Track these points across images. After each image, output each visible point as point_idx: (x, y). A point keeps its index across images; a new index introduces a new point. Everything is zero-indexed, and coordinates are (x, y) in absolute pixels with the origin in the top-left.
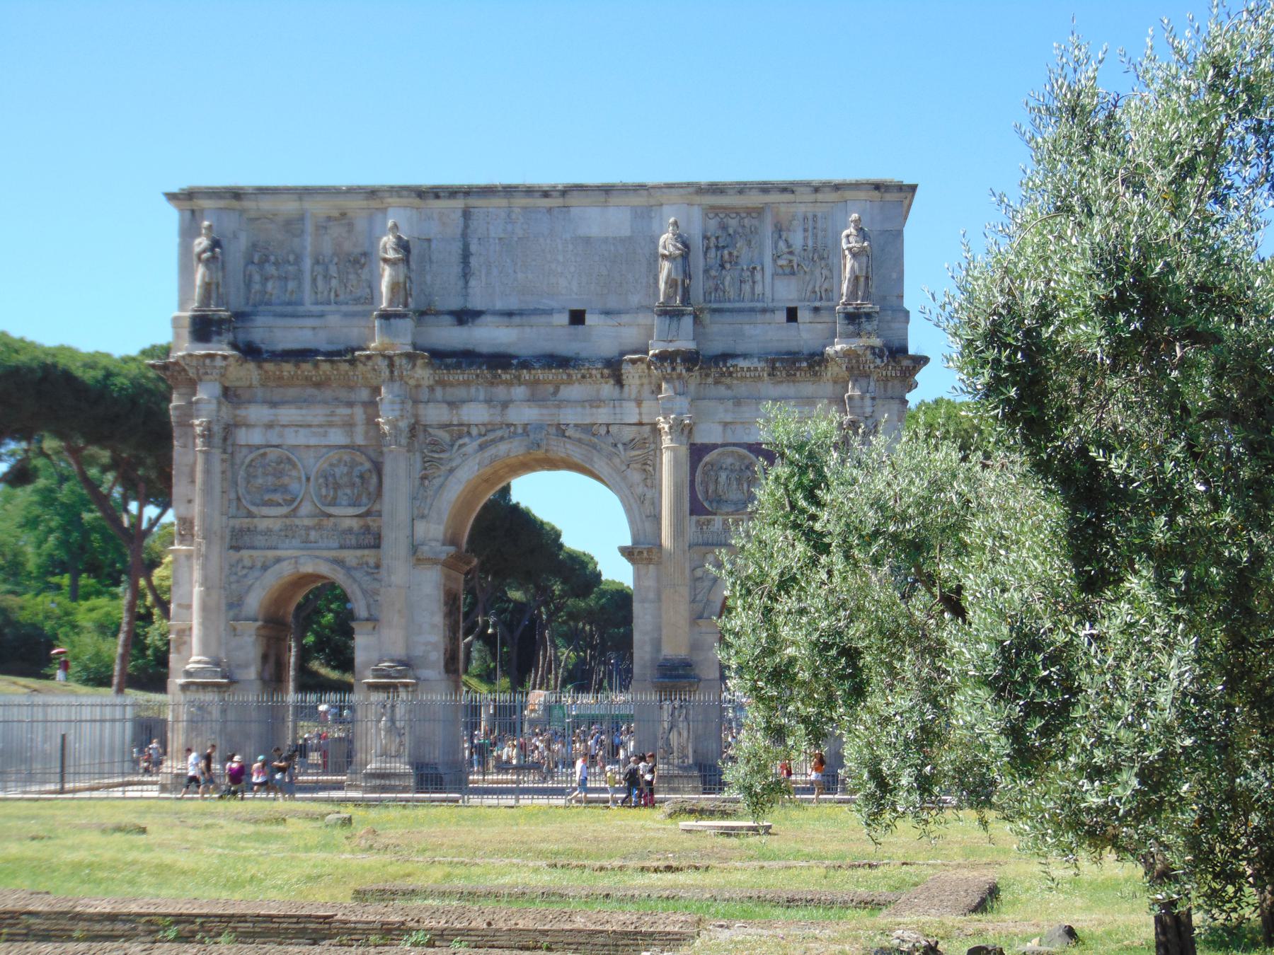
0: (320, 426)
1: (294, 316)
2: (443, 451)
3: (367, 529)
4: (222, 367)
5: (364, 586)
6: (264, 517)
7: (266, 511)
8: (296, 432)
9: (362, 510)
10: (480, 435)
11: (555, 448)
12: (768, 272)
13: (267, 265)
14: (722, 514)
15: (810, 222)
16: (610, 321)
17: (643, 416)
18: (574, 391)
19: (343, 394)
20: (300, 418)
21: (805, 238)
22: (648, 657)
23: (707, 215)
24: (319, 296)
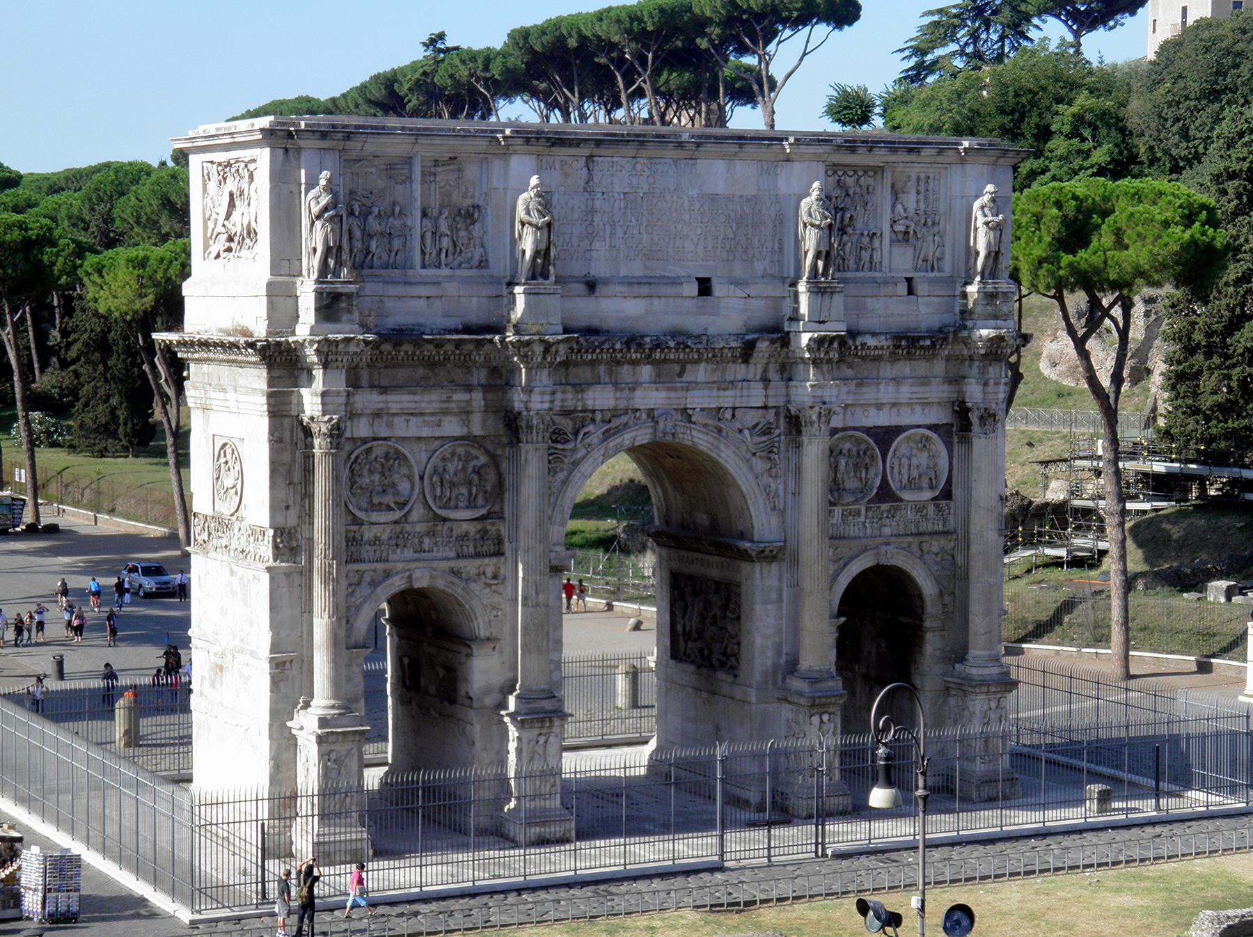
0: (432, 414)
1: (406, 283)
2: (567, 441)
3: (484, 533)
4: (355, 353)
6: (372, 524)
7: (375, 517)
8: (408, 421)
9: (483, 511)
10: (603, 421)
11: (681, 436)
12: (886, 241)
13: (371, 219)
14: (843, 505)
16: (740, 293)
17: (770, 399)
18: (701, 372)
19: (459, 375)
20: (412, 405)
21: (918, 201)
22: (769, 663)
24: (427, 257)
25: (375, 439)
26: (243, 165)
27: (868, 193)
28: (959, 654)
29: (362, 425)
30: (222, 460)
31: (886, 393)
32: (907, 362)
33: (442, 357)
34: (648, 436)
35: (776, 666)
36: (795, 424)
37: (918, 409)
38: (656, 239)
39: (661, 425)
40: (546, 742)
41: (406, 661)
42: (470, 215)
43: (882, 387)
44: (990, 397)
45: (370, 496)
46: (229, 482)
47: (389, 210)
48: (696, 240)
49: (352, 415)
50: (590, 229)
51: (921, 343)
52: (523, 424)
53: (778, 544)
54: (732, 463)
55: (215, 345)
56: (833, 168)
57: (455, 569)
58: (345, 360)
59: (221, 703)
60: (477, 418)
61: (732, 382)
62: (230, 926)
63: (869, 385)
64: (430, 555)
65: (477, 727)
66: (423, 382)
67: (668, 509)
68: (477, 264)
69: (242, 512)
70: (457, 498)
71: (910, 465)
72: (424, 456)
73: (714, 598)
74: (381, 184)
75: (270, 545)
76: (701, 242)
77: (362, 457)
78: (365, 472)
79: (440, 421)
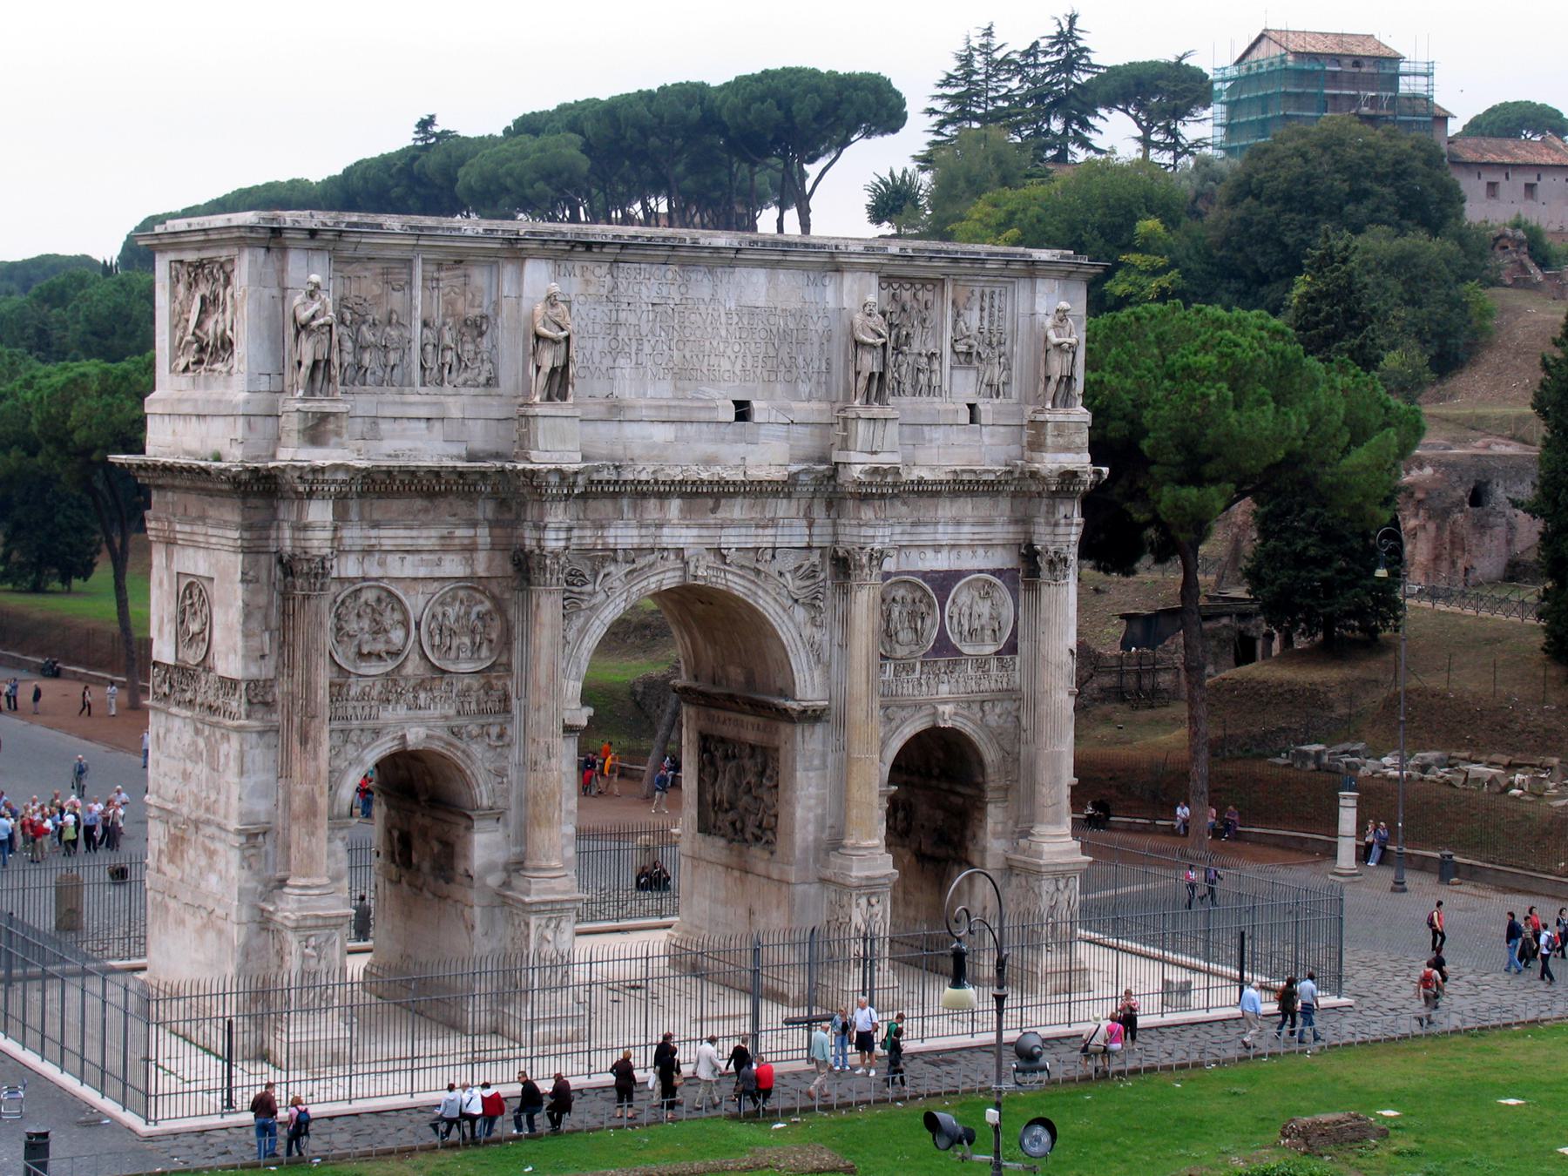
1: (403, 403)
3: (488, 688)
4: (344, 482)
5: (487, 765)
6: (360, 676)
8: (403, 559)
9: (488, 663)
11: (714, 579)
13: (364, 328)
15: (987, 299)
17: (815, 539)
18: (736, 510)
19: (462, 507)
20: (409, 542)
21: (982, 318)
22: (811, 838)
24: (428, 373)
25: (364, 579)
26: (217, 266)
27: (927, 308)
28: (1022, 831)
29: (350, 563)
30: (188, 602)
31: (944, 534)
33: (443, 488)
34: (677, 580)
35: (816, 840)
36: (843, 566)
37: (981, 551)
38: (688, 357)
39: (692, 568)
40: (557, 926)
41: (396, 834)
42: (477, 327)
43: (941, 529)
44: (1061, 539)
45: (359, 646)
46: (194, 627)
47: (385, 319)
48: (733, 357)
49: (340, 551)
50: (614, 344)
51: (985, 477)
52: (533, 563)
53: (822, 703)
54: (772, 611)
55: (182, 469)
56: (887, 279)
57: (456, 730)
58: (332, 489)
59: (182, 880)
60: (481, 559)
61: (772, 519)
62: (192, 1139)
63: (926, 524)
64: (428, 712)
65: (477, 910)
66: (421, 516)
67: (697, 664)
68: (482, 379)
69: (210, 662)
70: (458, 648)
72: (421, 601)
73: (748, 763)
74: (376, 290)
75: (244, 699)
77: (349, 600)
78: (353, 617)
79: (440, 560)
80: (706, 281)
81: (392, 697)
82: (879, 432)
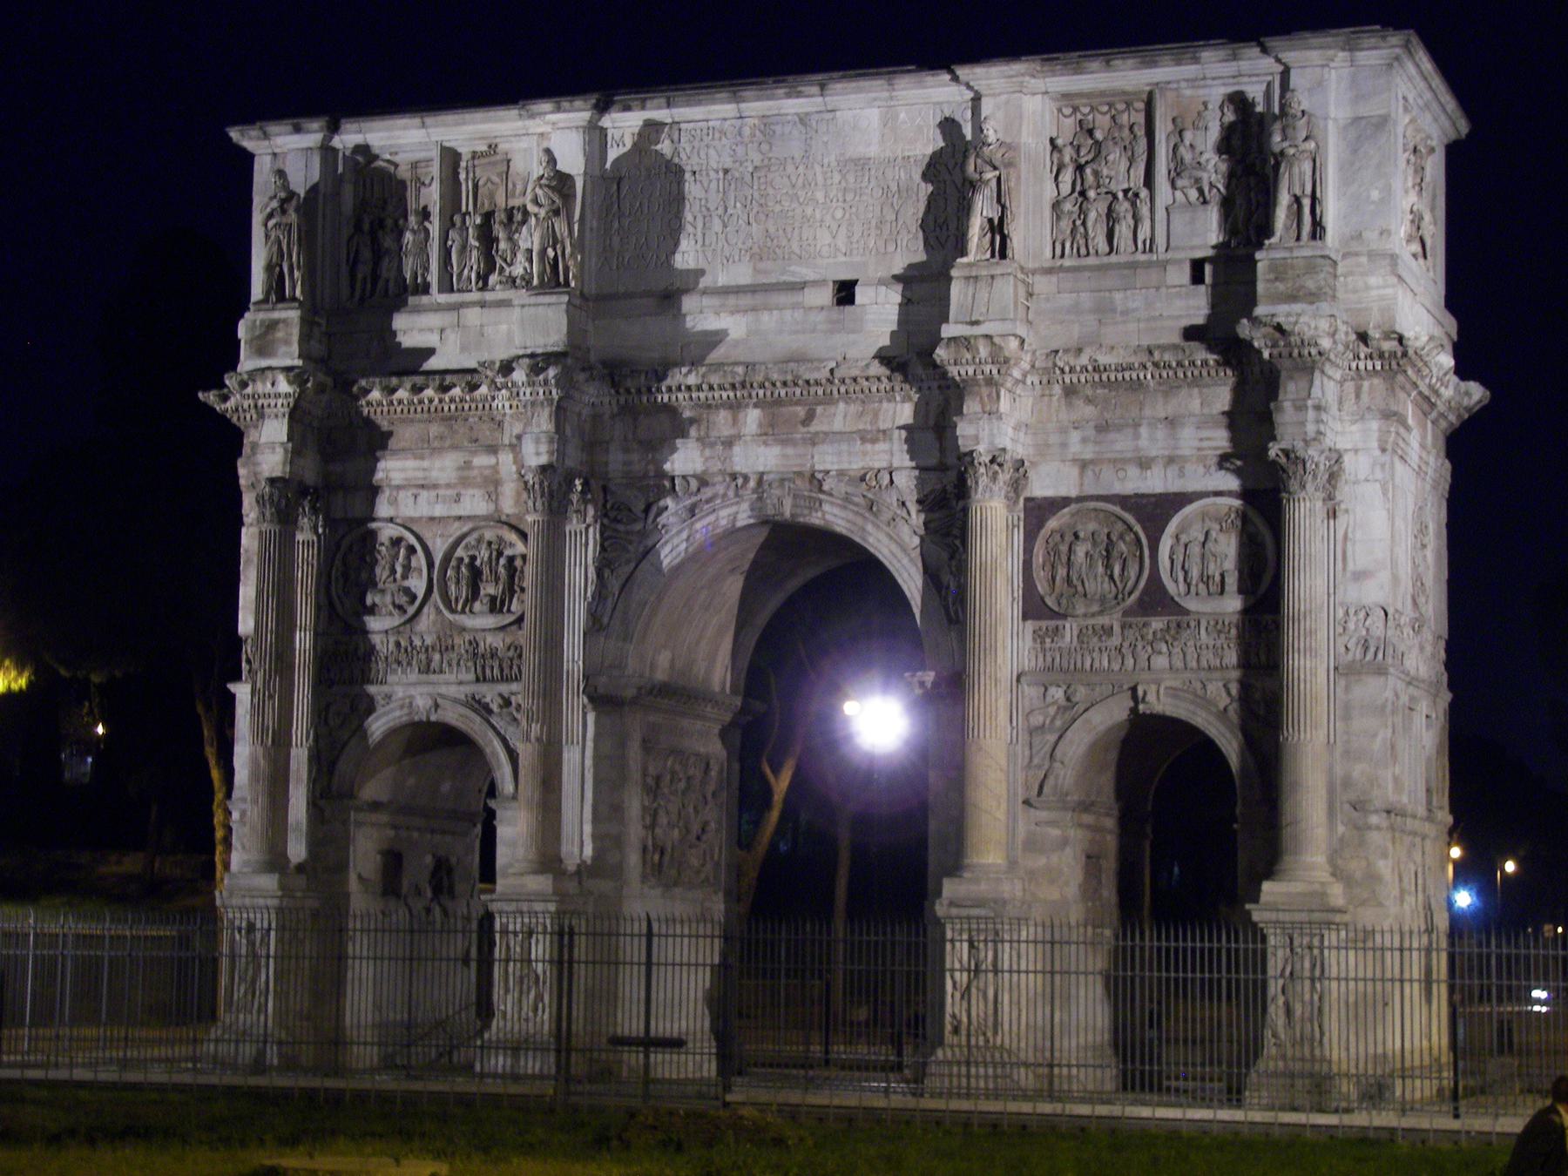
0: (448, 486)
2: (635, 521)
4: (287, 395)
18: (839, 417)
19: (485, 432)
20: (420, 474)
23: (1060, 110)
31: (1151, 441)
32: (1196, 390)
33: (453, 407)
38: (772, 230)
43: (1144, 431)
48: (834, 226)
54: (885, 551)
61: (884, 432)
64: (442, 677)
71: (1203, 556)
76: (843, 230)
79: (458, 495)
80: (795, 133)
81: (402, 657)
82: (983, 294)
